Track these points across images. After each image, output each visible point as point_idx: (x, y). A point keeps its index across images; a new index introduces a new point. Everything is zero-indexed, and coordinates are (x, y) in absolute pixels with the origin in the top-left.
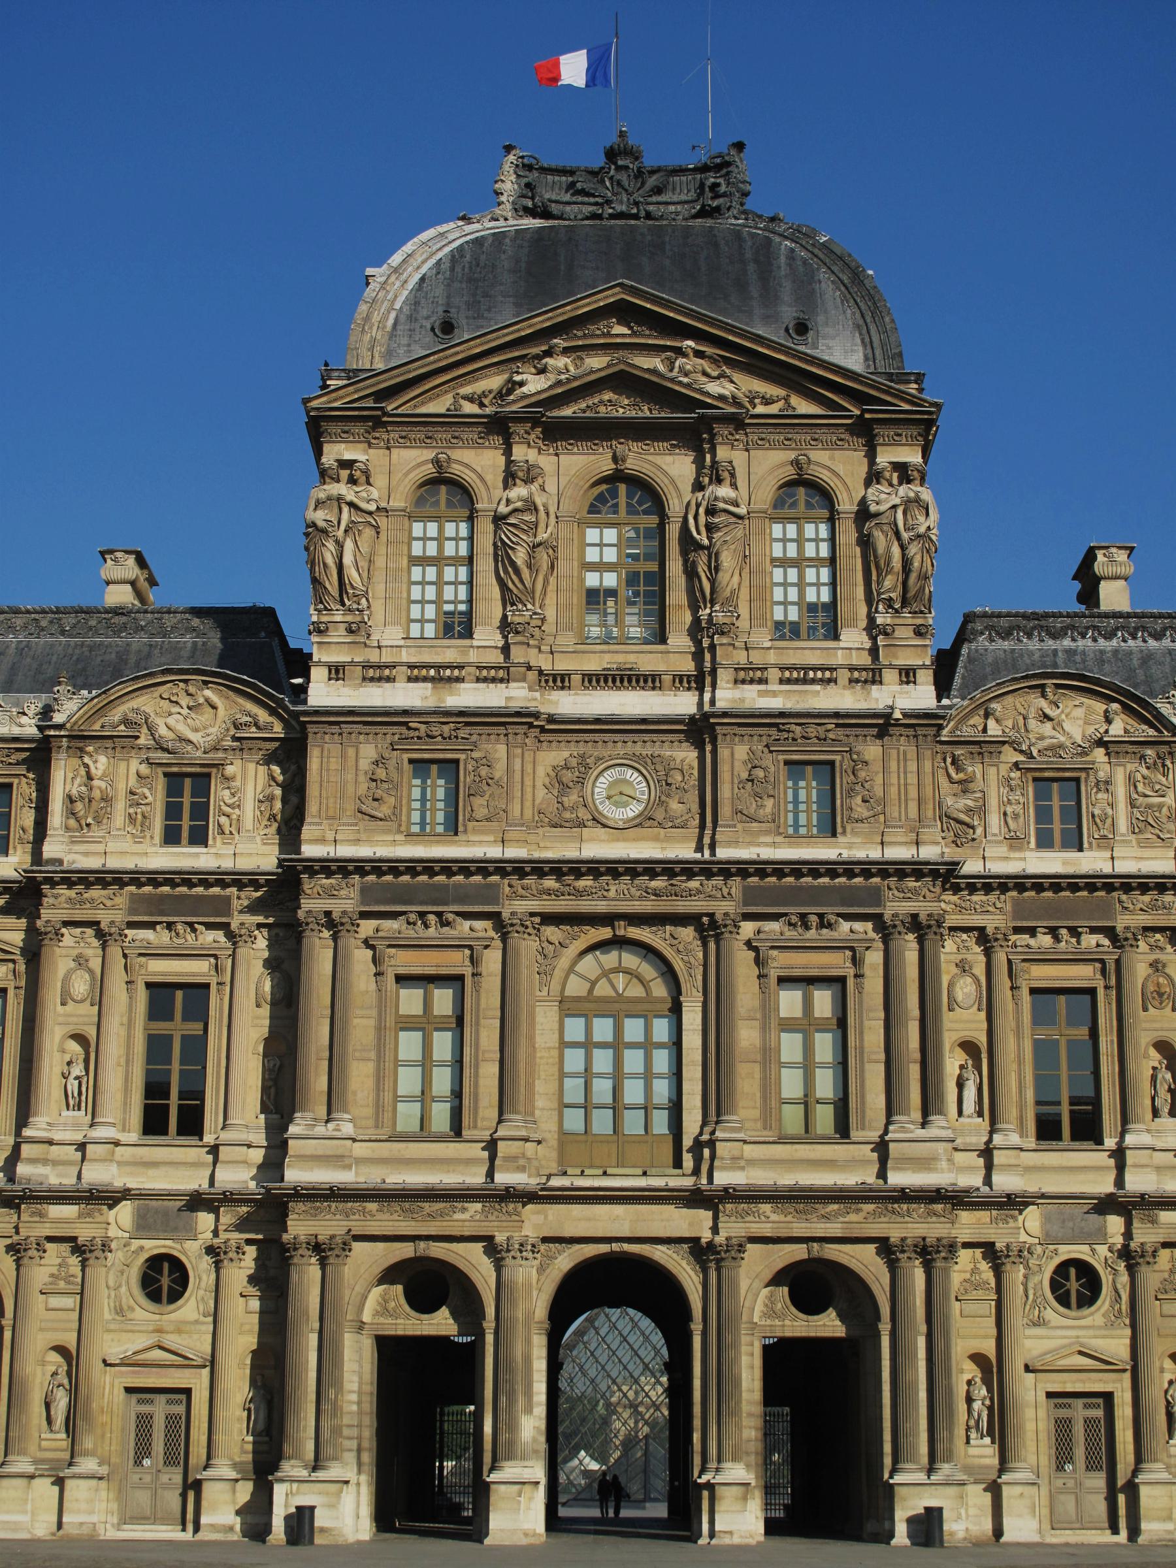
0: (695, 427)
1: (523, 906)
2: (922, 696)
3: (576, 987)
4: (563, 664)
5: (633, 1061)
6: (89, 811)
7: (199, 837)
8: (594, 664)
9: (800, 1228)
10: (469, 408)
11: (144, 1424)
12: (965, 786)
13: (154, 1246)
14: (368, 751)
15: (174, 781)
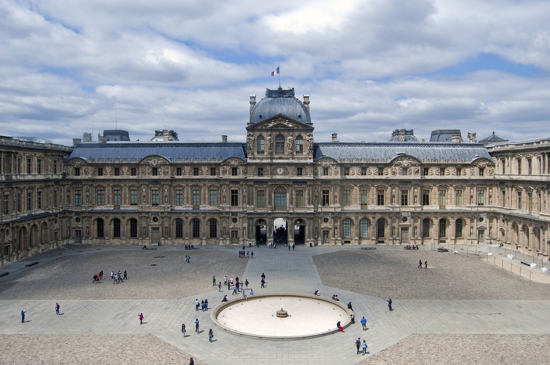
0: (289, 130)
1: (270, 184)
2: (312, 161)
3: (276, 191)
4: (275, 156)
5: (282, 199)
6: (224, 172)
7: (236, 175)
8: (277, 156)
9: (298, 216)
10: (264, 128)
11: (233, 234)
12: (316, 169)
13: (234, 217)
14: (254, 167)
15: (233, 169)
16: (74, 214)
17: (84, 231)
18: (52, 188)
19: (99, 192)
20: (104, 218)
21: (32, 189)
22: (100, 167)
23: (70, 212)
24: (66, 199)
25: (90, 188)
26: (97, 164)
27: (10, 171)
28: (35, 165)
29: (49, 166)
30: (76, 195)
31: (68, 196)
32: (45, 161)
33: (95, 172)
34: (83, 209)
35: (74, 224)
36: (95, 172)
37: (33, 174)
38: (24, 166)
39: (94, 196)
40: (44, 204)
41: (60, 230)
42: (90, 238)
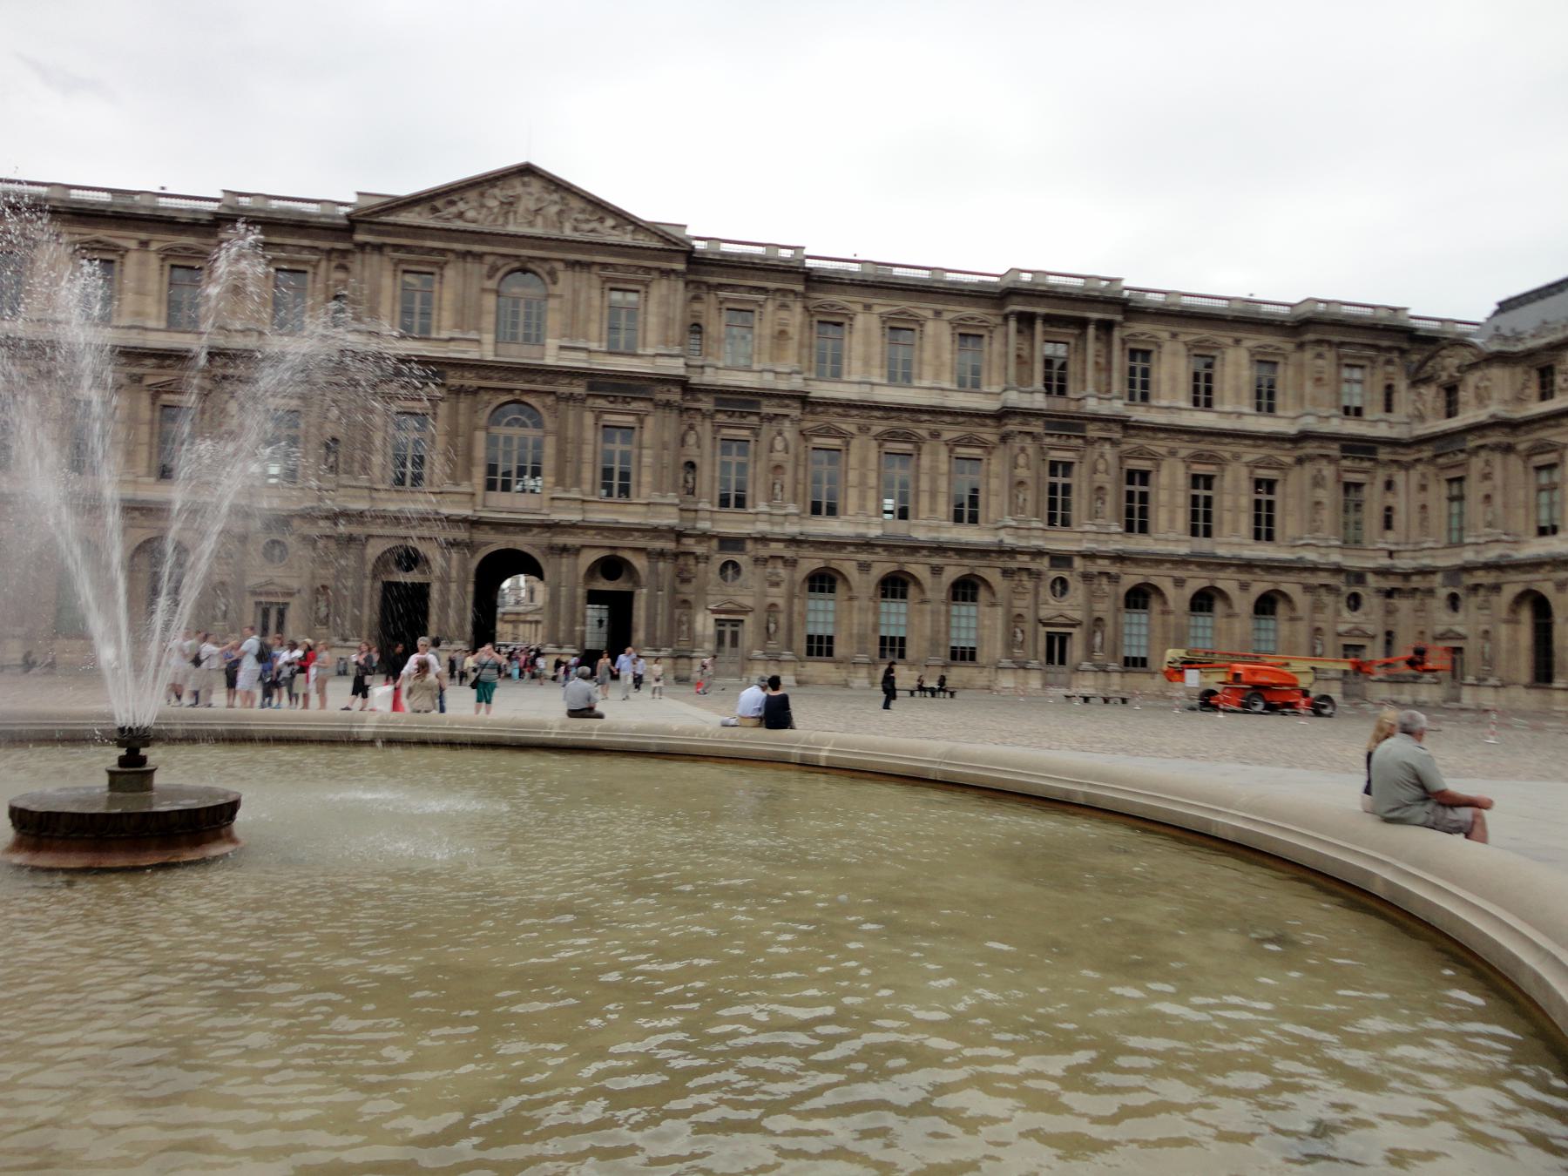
16: (1438, 579)
17: (1472, 647)
18: (1328, 471)
19: (1544, 478)
20: (1547, 589)
21: (1220, 462)
22: (1544, 360)
23: (1425, 572)
24: (1415, 518)
25: (1497, 458)
26: (1530, 354)
27: (1084, 389)
28: (1237, 377)
29: (1309, 387)
30: (1451, 499)
31: (1424, 507)
32: (1300, 367)
33: (1525, 387)
34: (1468, 555)
35: (1443, 619)
36: (1525, 387)
37: (1228, 408)
38: (1174, 378)
39: (1521, 494)
40: (1288, 522)
41: (1381, 641)
42: (1492, 681)
